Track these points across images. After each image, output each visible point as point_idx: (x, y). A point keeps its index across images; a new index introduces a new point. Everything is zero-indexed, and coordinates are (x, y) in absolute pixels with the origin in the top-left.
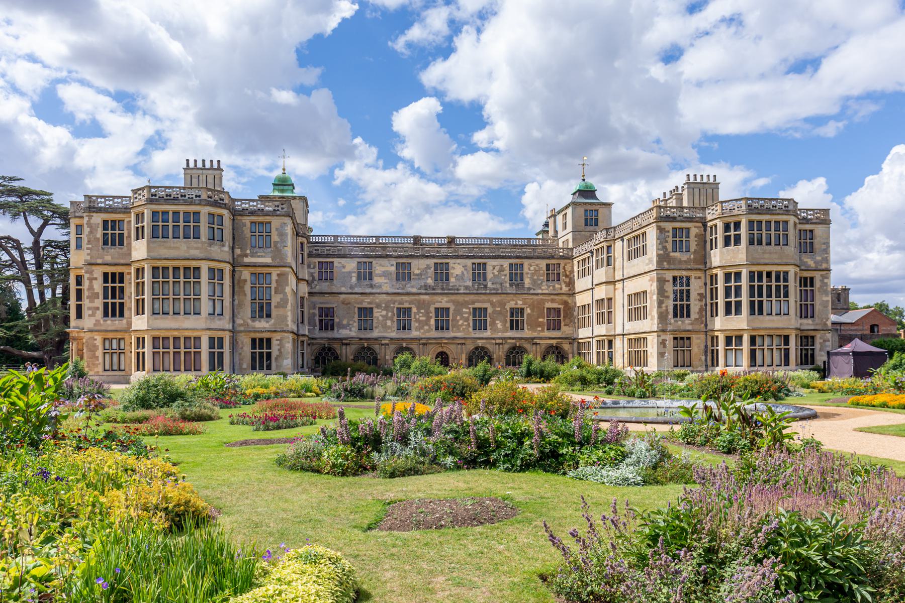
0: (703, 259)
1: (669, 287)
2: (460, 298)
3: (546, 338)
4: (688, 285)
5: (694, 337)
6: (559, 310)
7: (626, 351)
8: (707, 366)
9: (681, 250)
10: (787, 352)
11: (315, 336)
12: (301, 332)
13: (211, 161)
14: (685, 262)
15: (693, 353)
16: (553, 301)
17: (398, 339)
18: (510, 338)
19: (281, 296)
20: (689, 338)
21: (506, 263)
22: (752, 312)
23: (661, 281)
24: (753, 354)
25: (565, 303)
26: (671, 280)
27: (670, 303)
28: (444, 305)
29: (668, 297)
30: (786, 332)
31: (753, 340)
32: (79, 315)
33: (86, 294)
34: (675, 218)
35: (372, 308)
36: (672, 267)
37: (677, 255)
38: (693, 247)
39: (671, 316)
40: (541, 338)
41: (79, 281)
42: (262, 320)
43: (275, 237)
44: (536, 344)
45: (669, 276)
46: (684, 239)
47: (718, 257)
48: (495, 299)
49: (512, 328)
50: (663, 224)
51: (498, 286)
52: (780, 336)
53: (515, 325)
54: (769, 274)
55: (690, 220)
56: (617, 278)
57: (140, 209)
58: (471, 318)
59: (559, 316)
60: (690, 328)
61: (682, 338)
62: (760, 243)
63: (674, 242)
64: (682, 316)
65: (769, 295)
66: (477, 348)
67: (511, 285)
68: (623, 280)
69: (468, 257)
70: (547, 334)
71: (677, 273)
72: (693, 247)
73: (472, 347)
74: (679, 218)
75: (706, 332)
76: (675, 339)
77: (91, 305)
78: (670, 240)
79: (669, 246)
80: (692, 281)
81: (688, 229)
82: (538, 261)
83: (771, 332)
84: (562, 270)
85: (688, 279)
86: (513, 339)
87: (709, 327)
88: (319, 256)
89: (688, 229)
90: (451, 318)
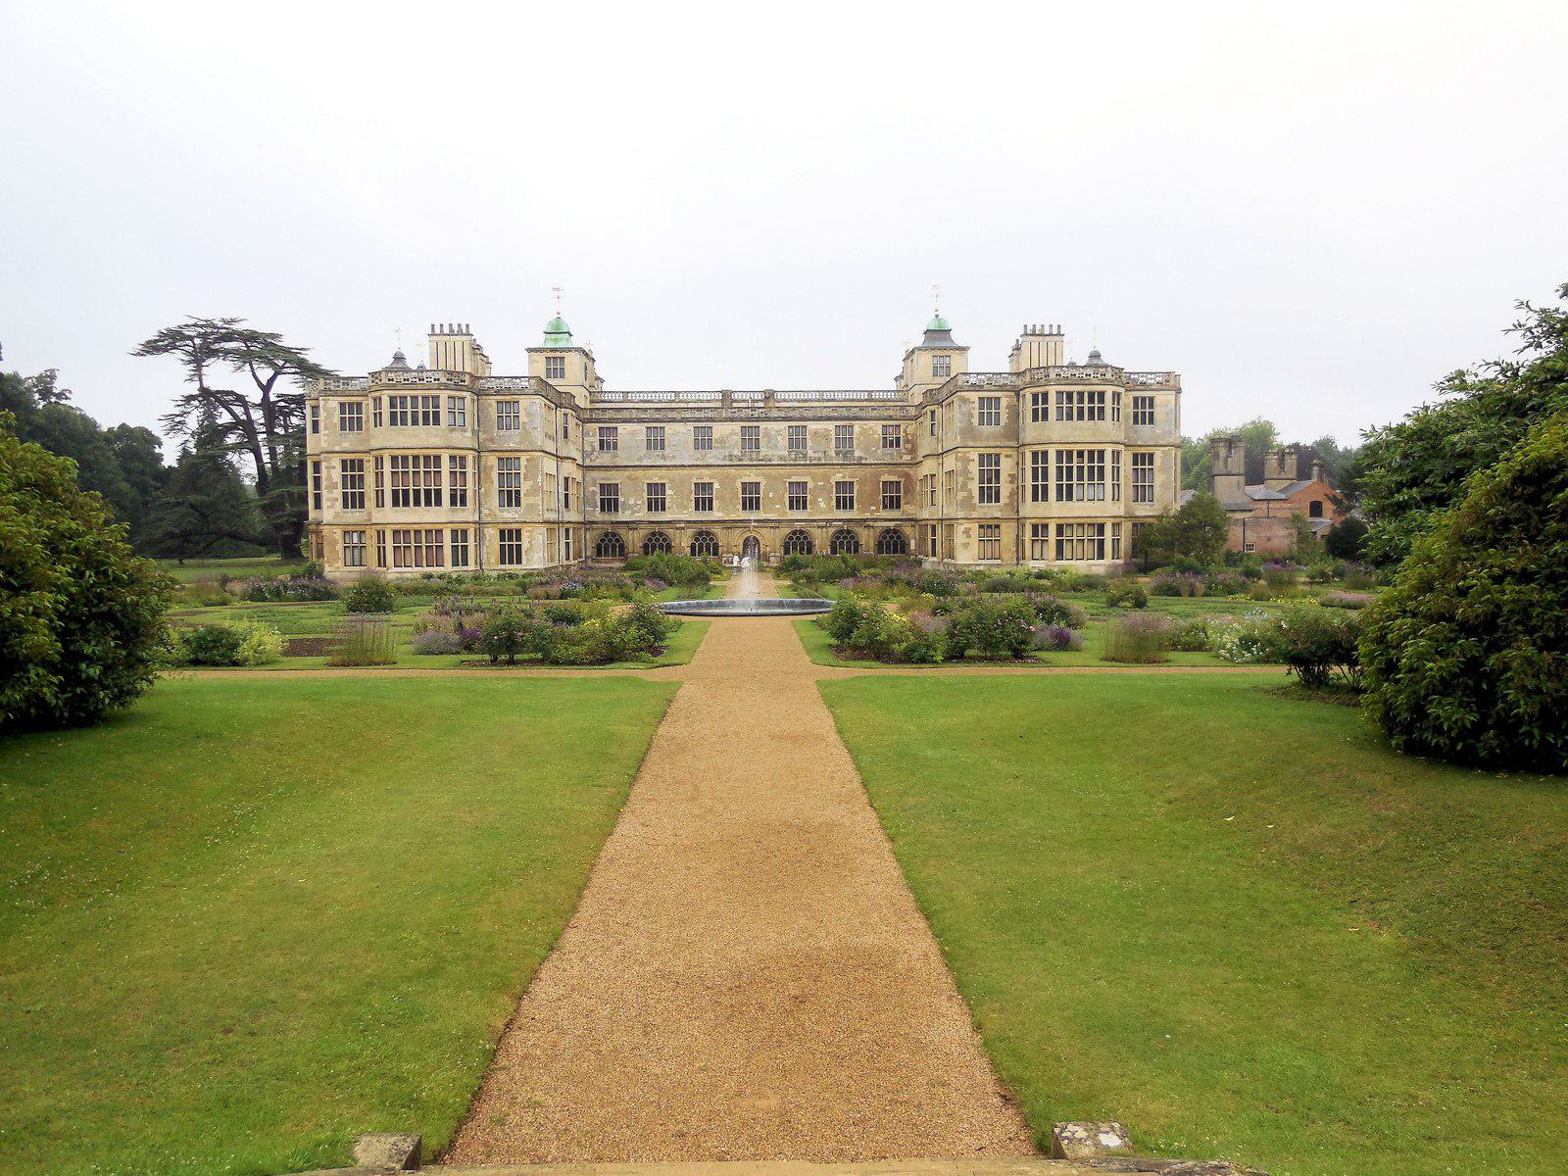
0: (1014, 432)
1: (974, 468)
2: (773, 471)
4: (997, 463)
5: (1003, 525)
6: (898, 483)
8: (1018, 558)
10: (1101, 543)
11: (594, 519)
12: (566, 519)
13: (459, 325)
14: (995, 437)
16: (890, 473)
17: (695, 522)
18: (836, 520)
19: (531, 483)
20: (997, 527)
21: (831, 426)
22: (1060, 498)
24: (1060, 544)
25: (907, 475)
26: (977, 459)
27: (975, 486)
28: (753, 479)
30: (1101, 521)
31: (1060, 529)
32: (318, 506)
33: (324, 483)
35: (663, 485)
36: (978, 444)
37: (987, 429)
38: (1004, 419)
40: (876, 520)
41: (317, 467)
43: (523, 418)
45: (974, 455)
46: (993, 411)
47: (1031, 431)
48: (814, 470)
49: (838, 507)
51: (821, 455)
52: (1094, 525)
53: (845, 503)
54: (1080, 454)
55: (1002, 388)
56: (940, 451)
57: (377, 394)
58: (787, 495)
61: (989, 527)
62: (1070, 417)
63: (981, 414)
65: (1080, 477)
66: (794, 533)
67: (837, 454)
69: (785, 419)
70: (884, 514)
72: (1004, 419)
73: (787, 531)
74: (986, 387)
75: (1018, 519)
76: (981, 527)
77: (330, 496)
79: (975, 421)
80: (1002, 460)
81: (999, 398)
83: (1082, 521)
84: (902, 434)
86: (840, 520)
87: (1021, 514)
90: (761, 495)
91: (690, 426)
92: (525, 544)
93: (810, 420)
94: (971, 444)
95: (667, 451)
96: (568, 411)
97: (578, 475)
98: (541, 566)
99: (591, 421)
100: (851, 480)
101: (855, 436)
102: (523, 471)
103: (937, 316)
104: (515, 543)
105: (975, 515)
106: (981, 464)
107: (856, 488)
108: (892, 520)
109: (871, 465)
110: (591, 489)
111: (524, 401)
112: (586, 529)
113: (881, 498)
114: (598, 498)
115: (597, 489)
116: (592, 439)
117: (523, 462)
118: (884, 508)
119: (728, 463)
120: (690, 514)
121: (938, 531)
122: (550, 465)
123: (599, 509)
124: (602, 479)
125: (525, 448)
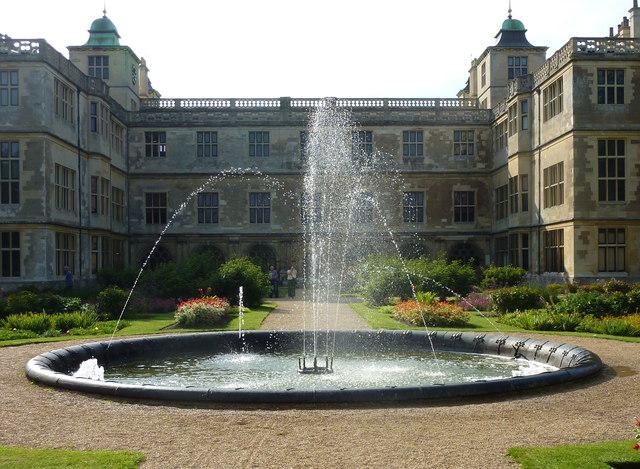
3: (454, 234)
4: (622, 151)
5: (629, 228)
6: (472, 193)
7: (542, 249)
9: (611, 101)
15: (628, 251)
16: (463, 182)
23: (580, 147)
25: (480, 185)
26: (595, 145)
29: (591, 170)
34: (601, 54)
36: (598, 126)
37: (608, 109)
38: (628, 96)
39: (595, 197)
40: (447, 234)
42: (6, 206)
44: (440, 241)
45: (593, 141)
50: (582, 64)
59: (472, 202)
60: (623, 215)
61: (612, 231)
63: (601, 92)
64: (612, 198)
67: (406, 161)
68: (539, 148)
70: (456, 227)
71: (604, 135)
76: (601, 231)
78: (595, 87)
79: (594, 98)
81: (621, 72)
82: (442, 129)
85: (621, 143)
88: (144, 124)
89: (621, 72)
91: (245, 131)
92: (24, 251)
93: (376, 125)
94: (589, 126)
95: (220, 158)
96: (97, 99)
97: (118, 182)
98: (44, 279)
99: (136, 125)
100: (421, 190)
101: (425, 142)
102: (22, 158)
103: (510, 17)
104: (11, 249)
105: (594, 215)
106: (601, 152)
107: (426, 198)
108: (465, 233)
109: (442, 173)
110: (136, 198)
111: (24, 71)
112: (131, 243)
113: (452, 209)
114: (144, 208)
115: (143, 199)
116: (137, 145)
117: (23, 147)
118: (455, 221)
119: (285, 171)
120: (244, 227)
121: (534, 240)
122: (70, 159)
123: (144, 221)
124: (148, 188)
125: (26, 129)
